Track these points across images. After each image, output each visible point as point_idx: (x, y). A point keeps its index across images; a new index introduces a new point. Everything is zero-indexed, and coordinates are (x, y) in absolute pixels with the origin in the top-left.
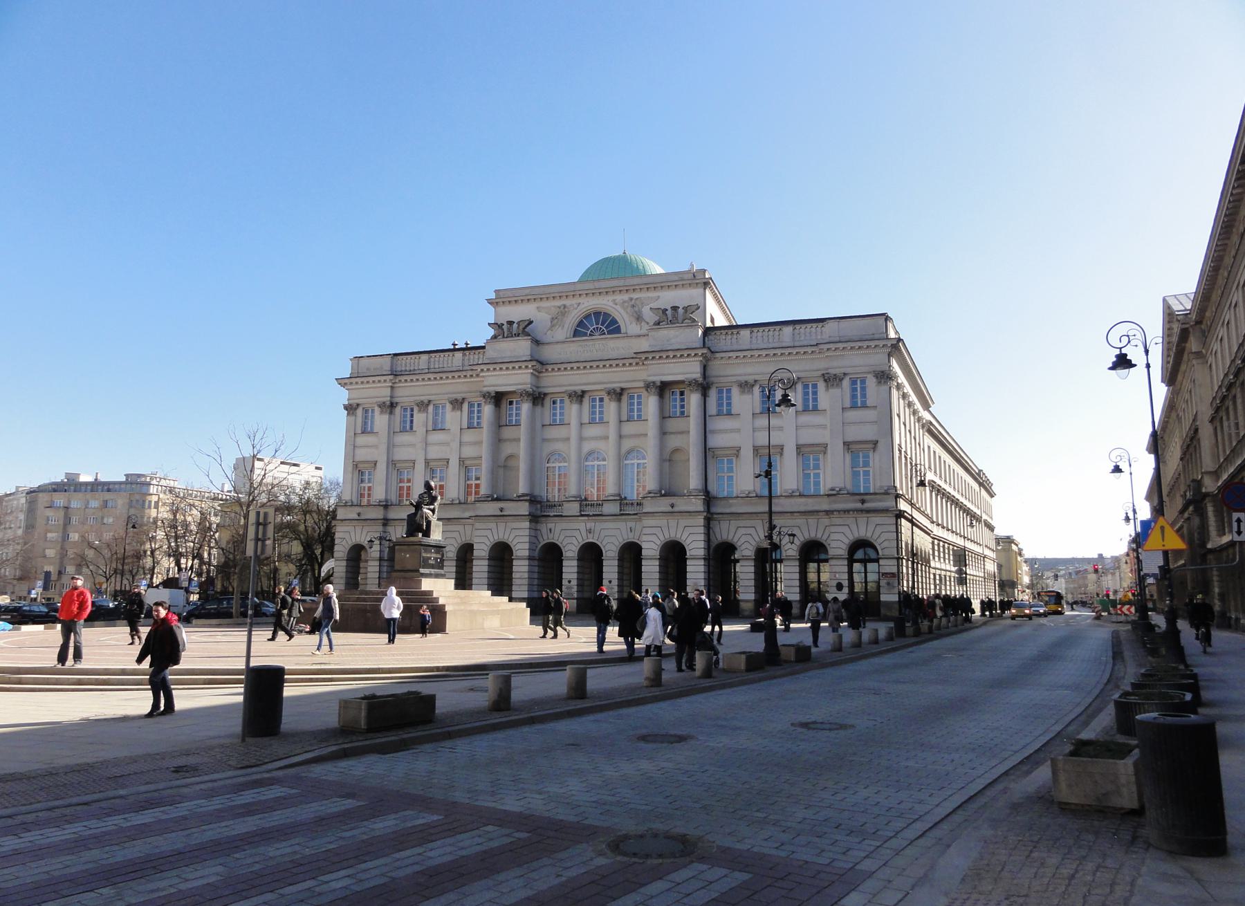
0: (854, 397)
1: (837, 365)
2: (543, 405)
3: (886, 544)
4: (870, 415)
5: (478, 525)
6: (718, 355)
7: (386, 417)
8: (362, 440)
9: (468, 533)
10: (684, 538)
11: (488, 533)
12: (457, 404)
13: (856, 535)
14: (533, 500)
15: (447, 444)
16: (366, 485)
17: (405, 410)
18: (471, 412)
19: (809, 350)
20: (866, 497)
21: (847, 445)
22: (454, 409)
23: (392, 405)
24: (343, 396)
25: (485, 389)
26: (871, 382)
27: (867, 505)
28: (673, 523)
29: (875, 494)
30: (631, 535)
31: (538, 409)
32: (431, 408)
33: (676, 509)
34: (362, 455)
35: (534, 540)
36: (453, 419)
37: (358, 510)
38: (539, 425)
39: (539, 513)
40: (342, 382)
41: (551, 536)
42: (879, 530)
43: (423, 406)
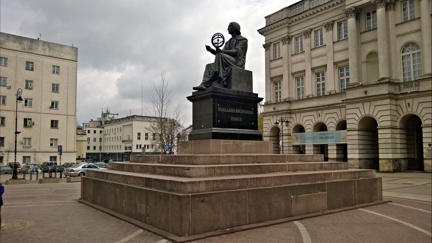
2: (394, 9)
5: (348, 106)
7: (286, 46)
8: (273, 64)
9: (343, 113)
11: (357, 111)
12: (329, 26)
14: (391, 83)
15: (325, 55)
16: (278, 91)
17: (297, 39)
18: (339, 30)
22: (327, 30)
23: (289, 39)
24: (262, 39)
25: (347, 7)
31: (391, 13)
32: (313, 34)
34: (274, 73)
35: (395, 113)
36: (329, 37)
37: (274, 106)
38: (392, 25)
39: (398, 92)
40: (261, 32)
41: (409, 109)
43: (307, 34)
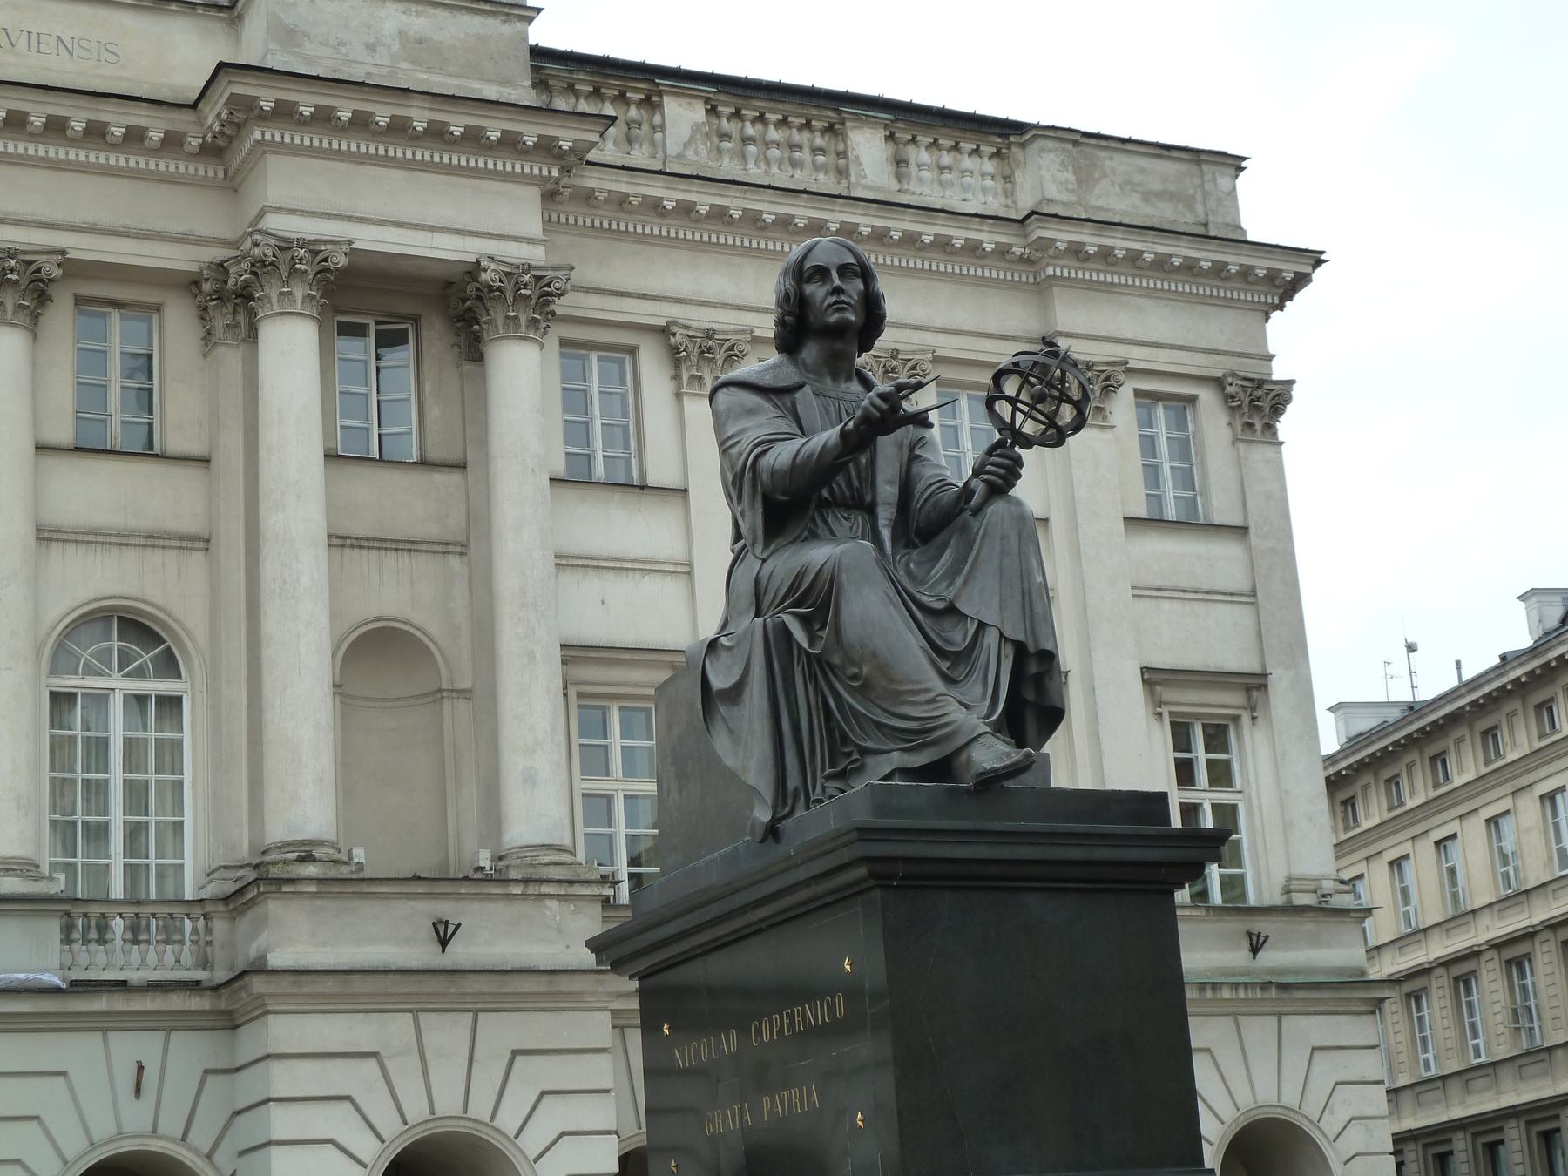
0: (1152, 475)
1: (1092, 325)
3: (1355, 1139)
4: (1218, 561)
6: (591, 180)
10: (509, 1120)
13: (1245, 1100)
19: (989, 238)
20: (1261, 925)
21: (1153, 678)
26: (1213, 421)
27: (1270, 958)
28: (447, 1034)
29: (1290, 910)
30: (137, 1116)
33: (461, 953)
42: (1328, 1070)
